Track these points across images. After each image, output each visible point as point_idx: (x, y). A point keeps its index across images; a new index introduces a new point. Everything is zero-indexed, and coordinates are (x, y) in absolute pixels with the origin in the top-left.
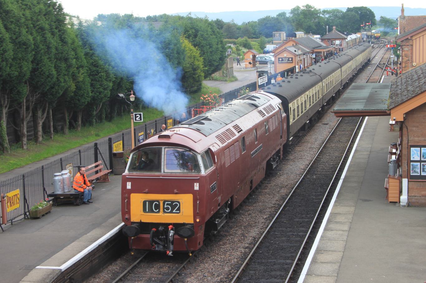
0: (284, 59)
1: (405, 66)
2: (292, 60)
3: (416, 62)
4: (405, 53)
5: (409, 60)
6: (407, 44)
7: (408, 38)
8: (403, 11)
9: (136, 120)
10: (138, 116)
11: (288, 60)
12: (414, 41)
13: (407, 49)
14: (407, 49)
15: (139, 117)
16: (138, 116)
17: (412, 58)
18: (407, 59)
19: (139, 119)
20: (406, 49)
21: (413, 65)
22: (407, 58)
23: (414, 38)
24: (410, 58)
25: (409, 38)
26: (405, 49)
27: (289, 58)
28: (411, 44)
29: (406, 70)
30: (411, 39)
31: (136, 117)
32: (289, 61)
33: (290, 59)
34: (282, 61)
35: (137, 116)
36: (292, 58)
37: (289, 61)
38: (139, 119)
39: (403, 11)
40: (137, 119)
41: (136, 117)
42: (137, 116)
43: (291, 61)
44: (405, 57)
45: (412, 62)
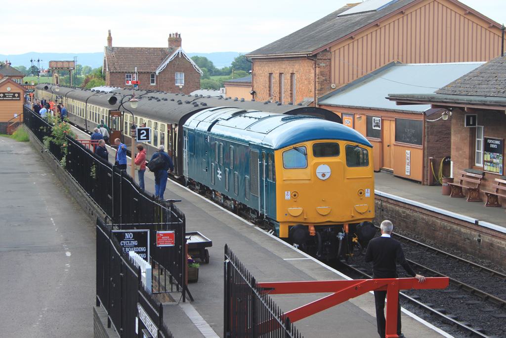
0: (7, 94)
1: (321, 88)
2: (19, 96)
3: (335, 83)
4: (322, 70)
5: (326, 80)
6: (324, 58)
7: (326, 49)
8: (110, 39)
9: (139, 139)
10: (143, 133)
11: (14, 96)
12: (333, 53)
13: (324, 65)
14: (324, 65)
15: (145, 134)
16: (143, 133)
17: (330, 77)
18: (324, 78)
19: (145, 138)
20: (322, 65)
21: (332, 86)
22: (324, 76)
23: (332, 50)
24: (328, 77)
25: (328, 50)
26: (321, 65)
27: (14, 93)
28: (329, 58)
29: (323, 94)
30: (329, 51)
31: (140, 134)
32: (15, 97)
33: (16, 95)
34: (3, 97)
35: (142, 132)
36: (19, 94)
37: (15, 97)
38: (145, 138)
39: (110, 39)
40: (142, 137)
41: (140, 134)
42: (142, 132)
43: (17, 97)
44: (321, 75)
45: (330, 83)
